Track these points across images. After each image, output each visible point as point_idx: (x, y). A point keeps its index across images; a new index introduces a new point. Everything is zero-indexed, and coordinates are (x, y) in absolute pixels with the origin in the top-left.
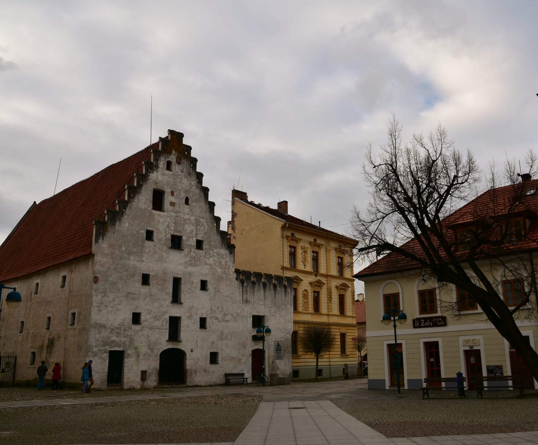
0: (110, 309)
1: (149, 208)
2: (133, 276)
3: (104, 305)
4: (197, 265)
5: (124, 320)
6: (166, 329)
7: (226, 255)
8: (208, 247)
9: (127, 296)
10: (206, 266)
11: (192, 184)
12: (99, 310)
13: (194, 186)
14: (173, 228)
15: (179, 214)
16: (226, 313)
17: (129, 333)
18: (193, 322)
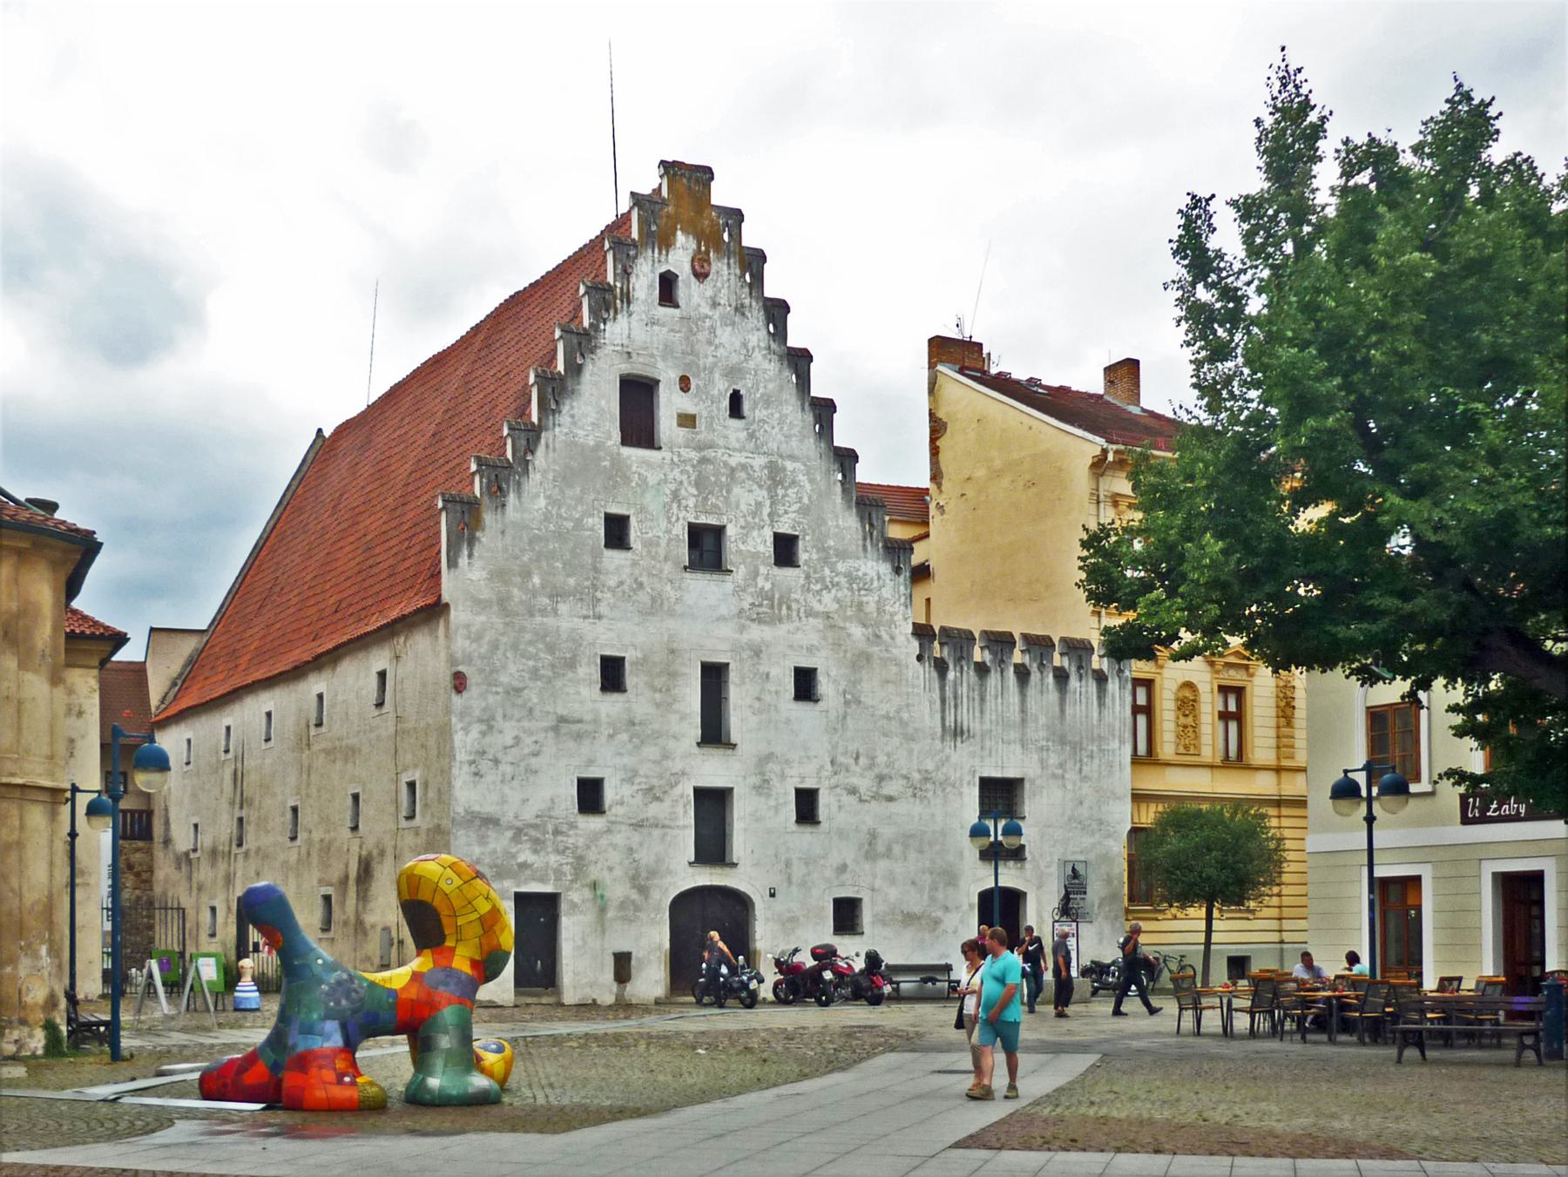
0: (509, 769)
2: (572, 664)
3: (491, 757)
4: (780, 620)
8: (815, 556)
9: (555, 729)
10: (811, 619)
16: (885, 771)
17: (571, 841)
18: (772, 803)
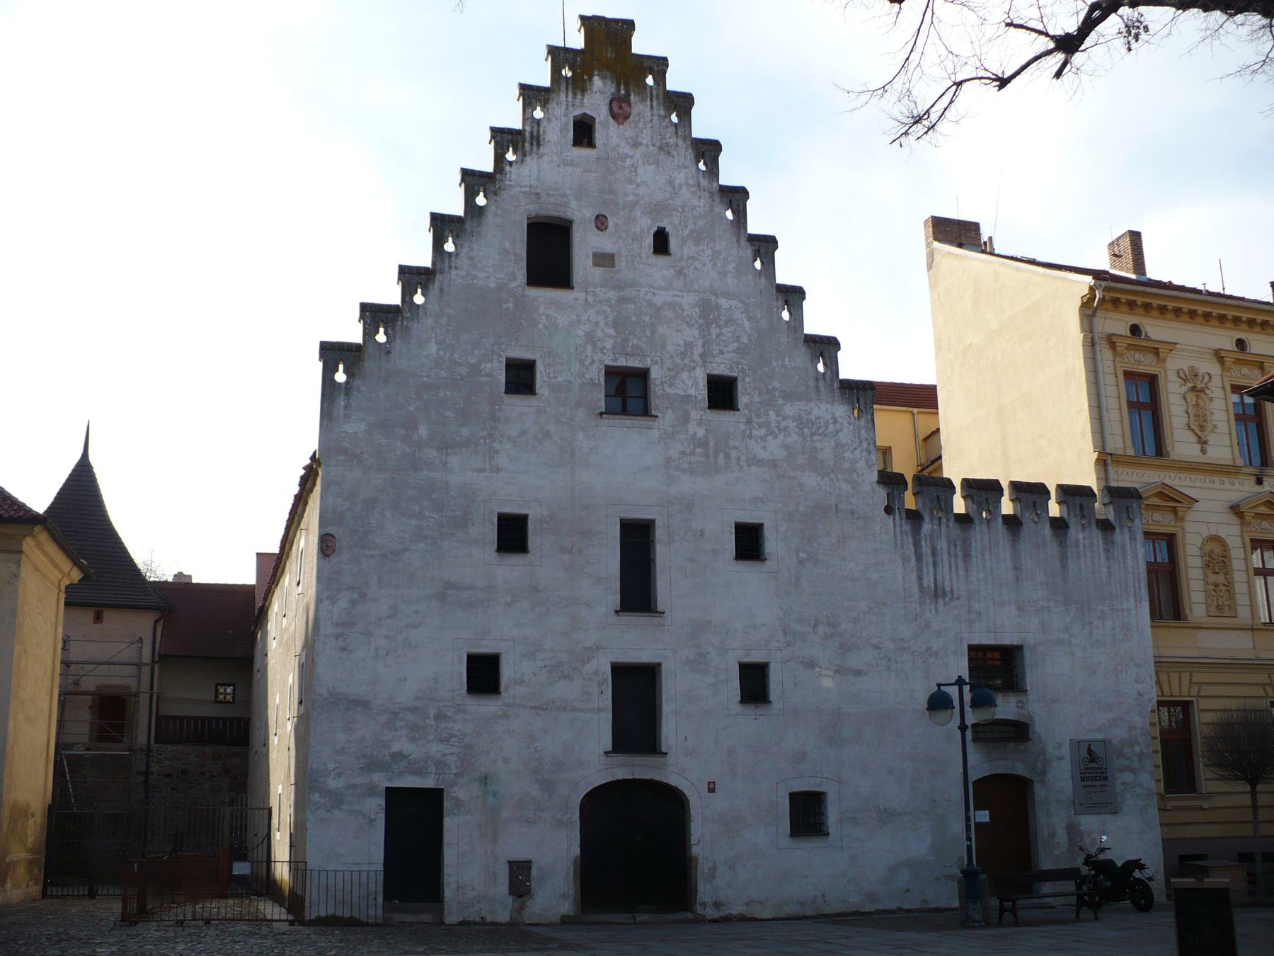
1: (513, 284)
2: (463, 522)
5: (436, 680)
6: (600, 710)
7: (835, 422)
8: (757, 399)
9: (442, 597)
10: (754, 468)
11: (677, 182)
12: (343, 649)
13: (685, 187)
14: (608, 344)
15: (631, 293)
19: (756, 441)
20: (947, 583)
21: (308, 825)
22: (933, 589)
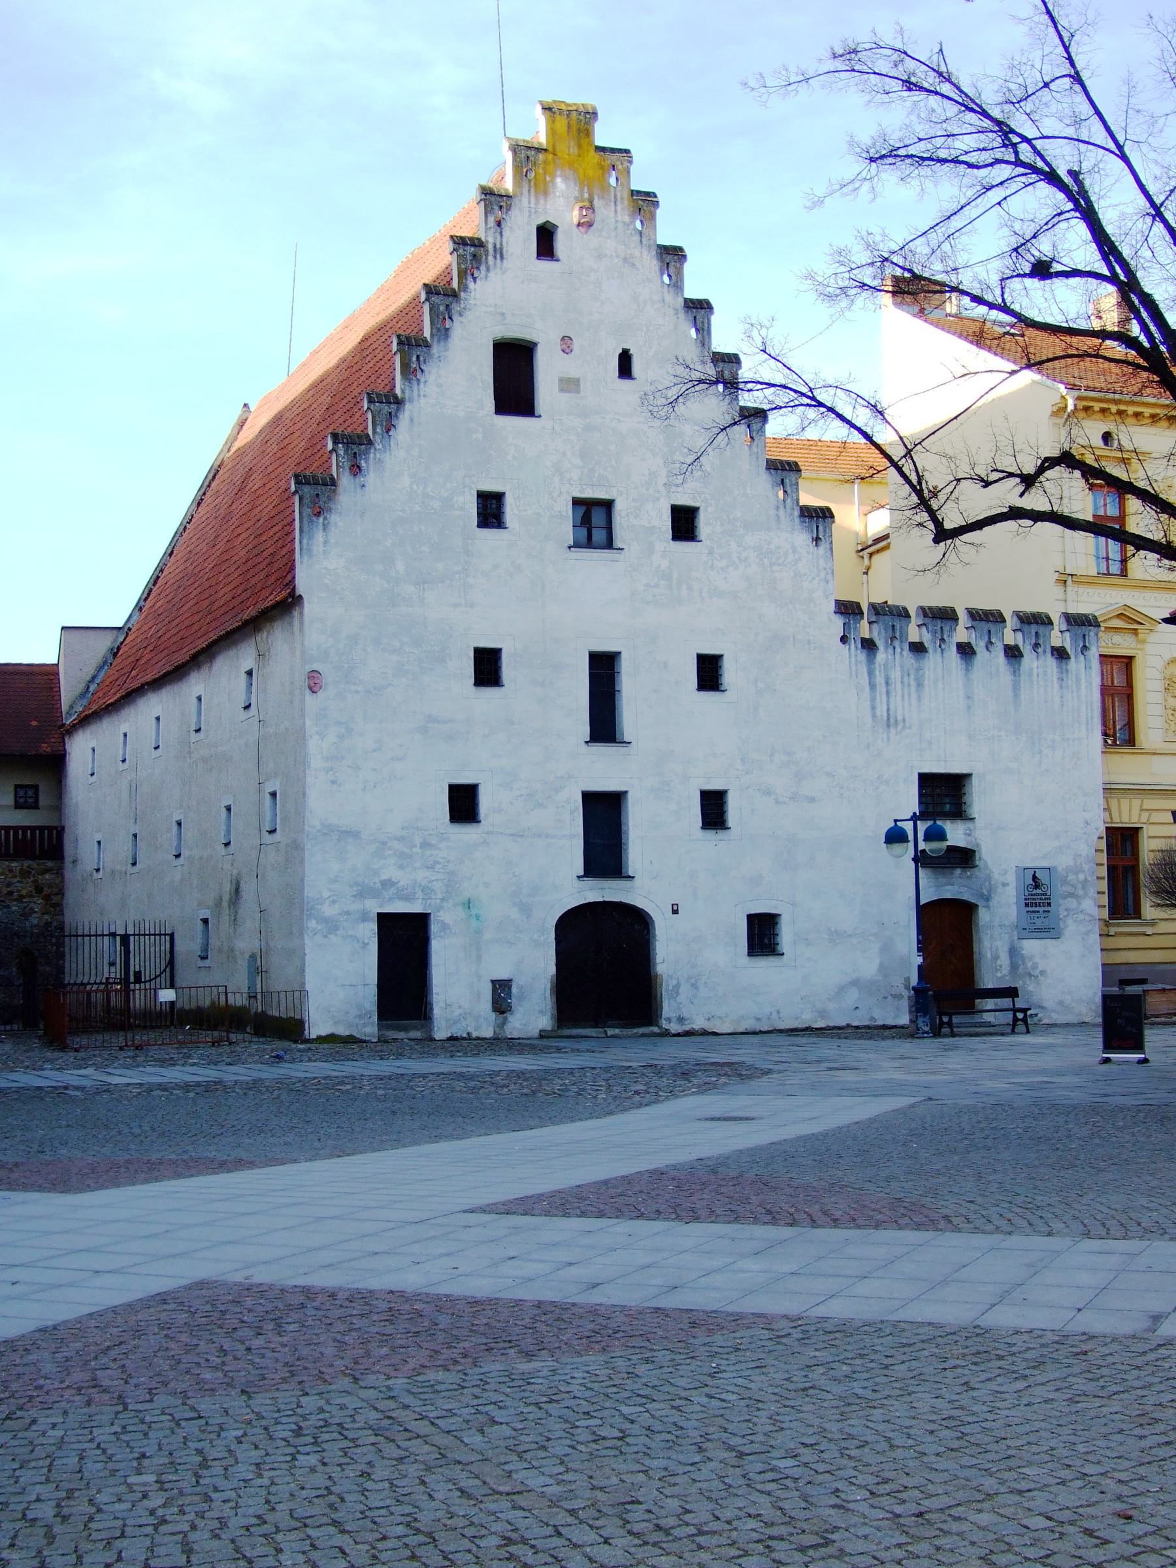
6: (573, 836)
7: (794, 552)
12: (333, 782)
19: (718, 572)
20: (900, 712)
21: (307, 951)
22: (885, 718)
